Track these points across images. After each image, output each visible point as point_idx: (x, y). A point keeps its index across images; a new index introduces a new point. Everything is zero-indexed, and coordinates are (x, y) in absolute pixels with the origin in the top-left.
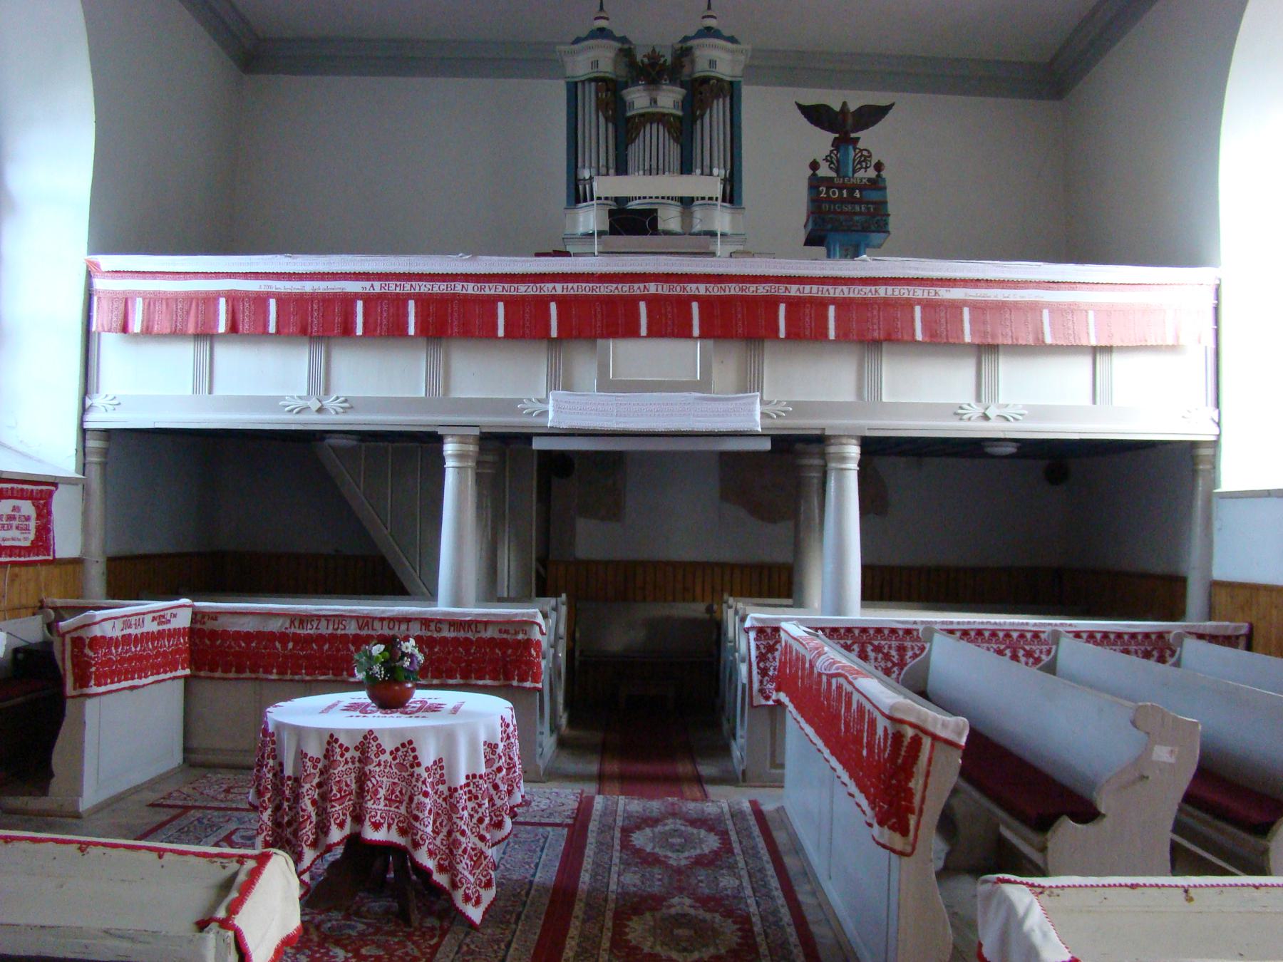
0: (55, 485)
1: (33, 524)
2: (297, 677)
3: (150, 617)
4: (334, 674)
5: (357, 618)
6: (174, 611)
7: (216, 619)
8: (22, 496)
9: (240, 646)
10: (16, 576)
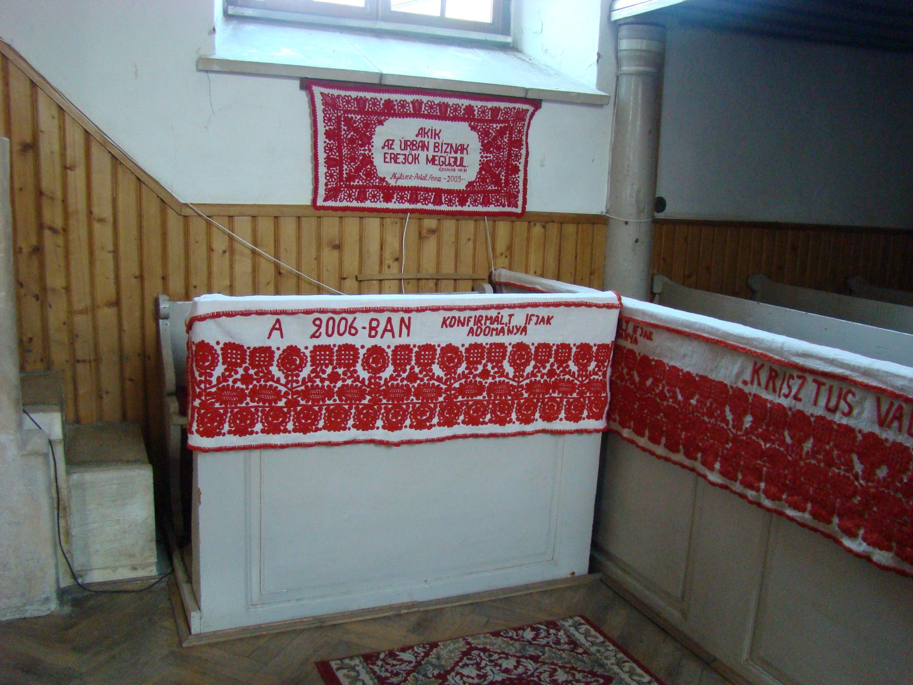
0: (536, 104)
1: (473, 160)
2: (751, 494)
3: (440, 316)
4: (814, 514)
5: (878, 393)
6: (543, 312)
7: (649, 337)
8: (443, 114)
9: (674, 396)
10: (432, 232)
